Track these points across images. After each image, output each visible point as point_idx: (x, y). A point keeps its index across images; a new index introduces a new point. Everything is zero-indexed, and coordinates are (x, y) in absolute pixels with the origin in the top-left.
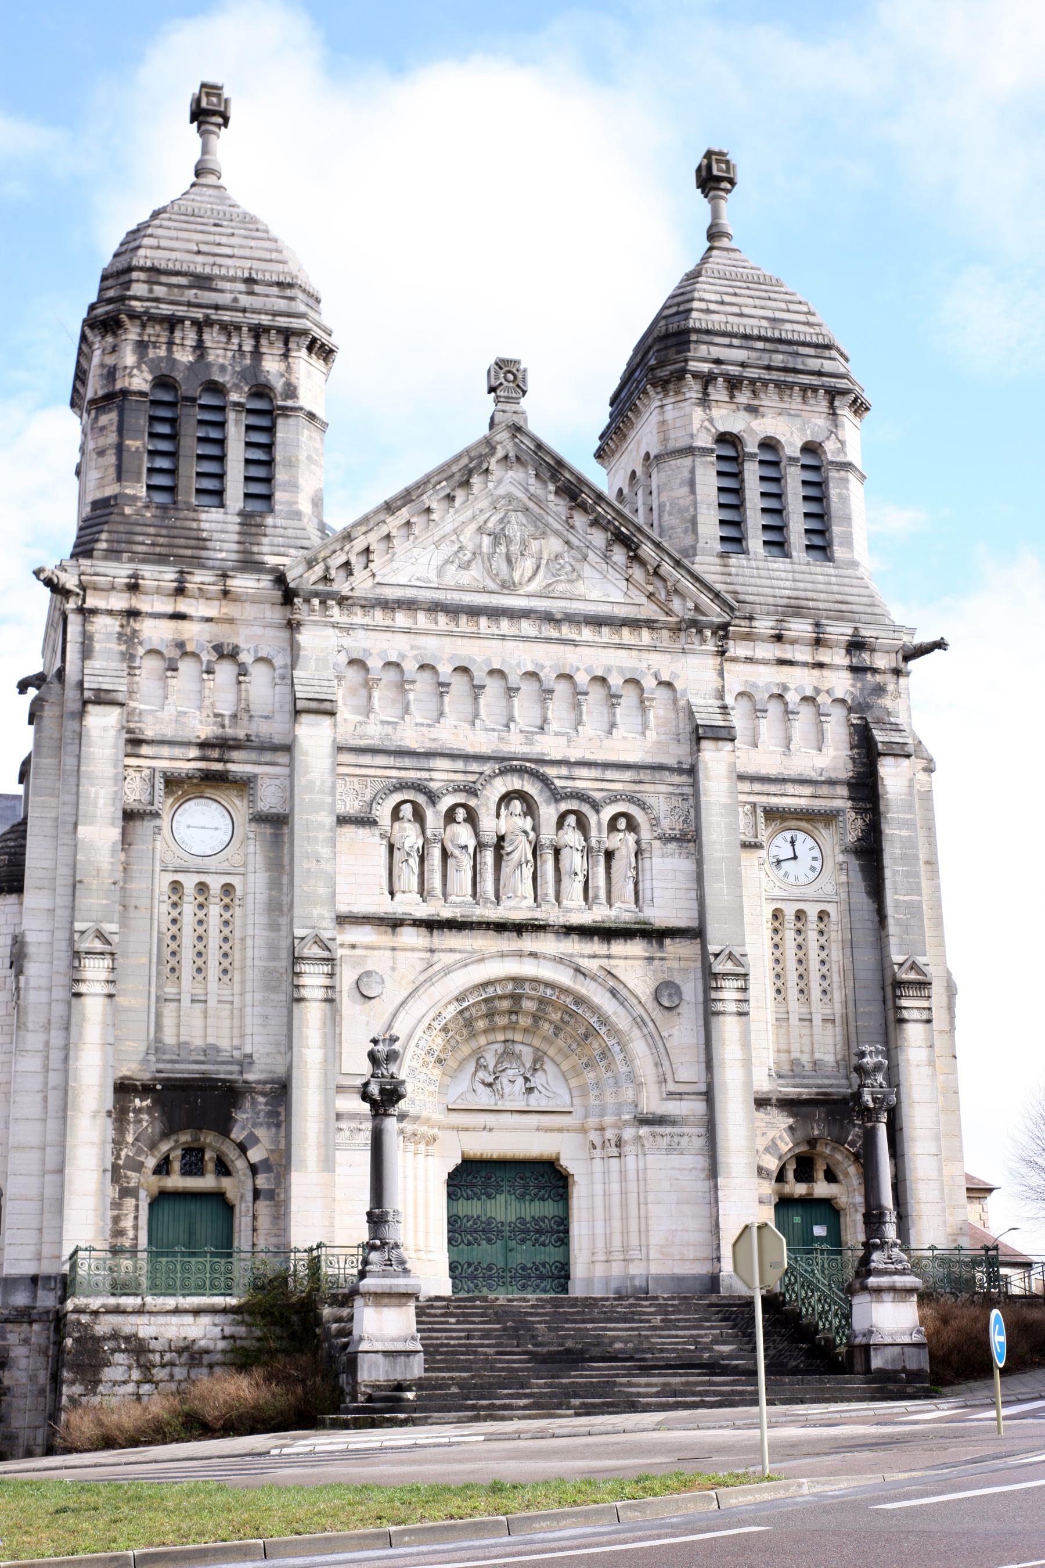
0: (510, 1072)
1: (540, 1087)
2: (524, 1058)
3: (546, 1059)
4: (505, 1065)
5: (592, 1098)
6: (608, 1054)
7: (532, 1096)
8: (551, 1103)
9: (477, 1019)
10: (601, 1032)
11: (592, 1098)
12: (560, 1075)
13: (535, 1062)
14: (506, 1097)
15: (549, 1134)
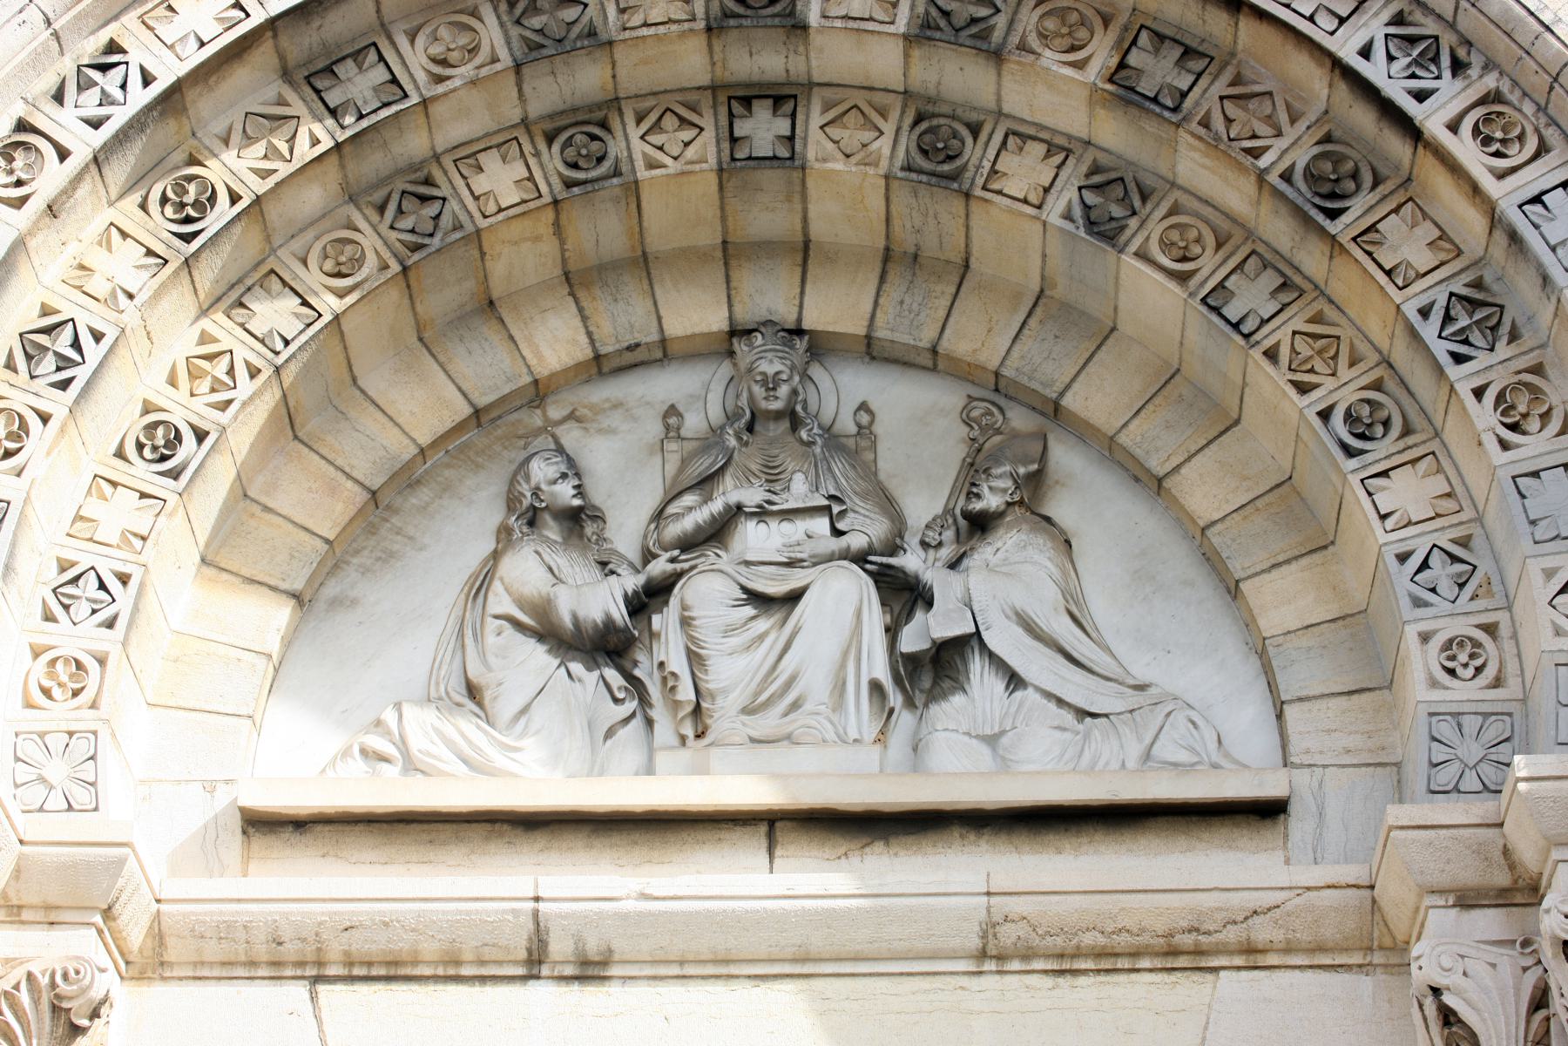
0: (755, 539)
1: (1003, 639)
2: (889, 462)
3: (1065, 457)
4: (730, 492)
5: (1420, 663)
6: (1520, 295)
7: (951, 712)
8: (1103, 744)
9: (469, 155)
10: (1432, 118)
11: (1420, 663)
12: (1179, 561)
13: (973, 471)
14: (725, 716)
15: (1087, 990)
